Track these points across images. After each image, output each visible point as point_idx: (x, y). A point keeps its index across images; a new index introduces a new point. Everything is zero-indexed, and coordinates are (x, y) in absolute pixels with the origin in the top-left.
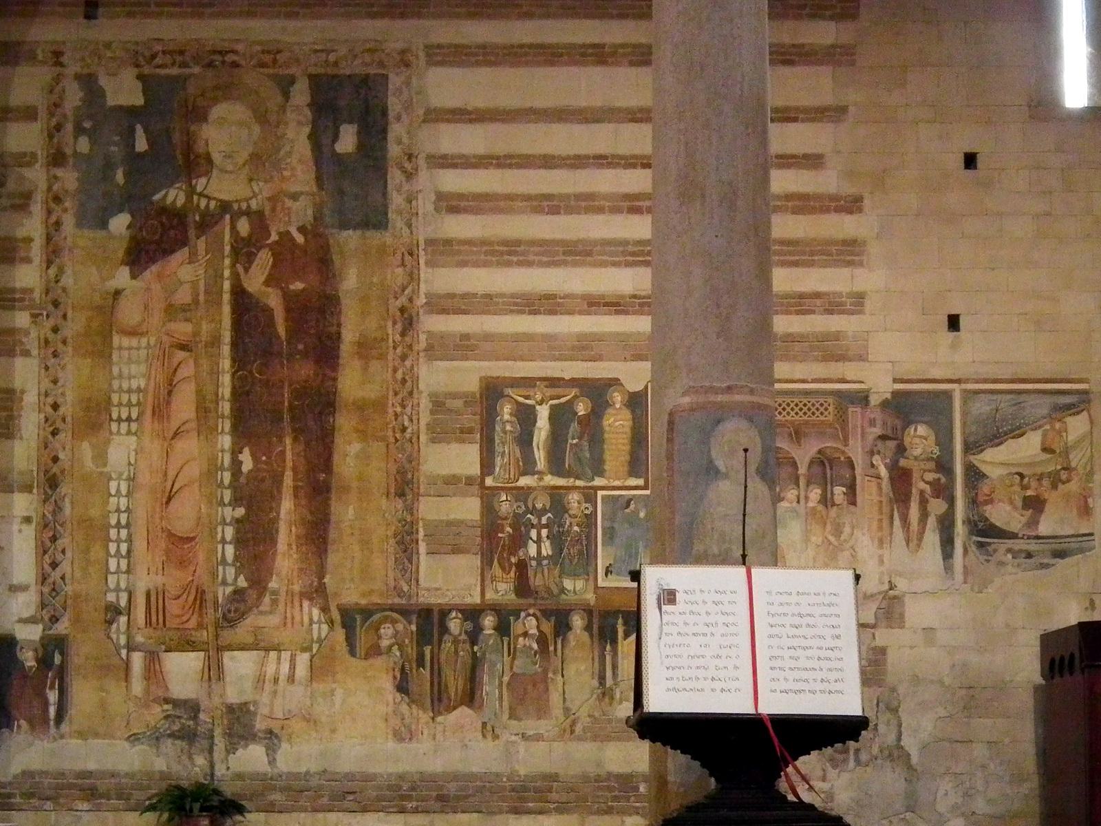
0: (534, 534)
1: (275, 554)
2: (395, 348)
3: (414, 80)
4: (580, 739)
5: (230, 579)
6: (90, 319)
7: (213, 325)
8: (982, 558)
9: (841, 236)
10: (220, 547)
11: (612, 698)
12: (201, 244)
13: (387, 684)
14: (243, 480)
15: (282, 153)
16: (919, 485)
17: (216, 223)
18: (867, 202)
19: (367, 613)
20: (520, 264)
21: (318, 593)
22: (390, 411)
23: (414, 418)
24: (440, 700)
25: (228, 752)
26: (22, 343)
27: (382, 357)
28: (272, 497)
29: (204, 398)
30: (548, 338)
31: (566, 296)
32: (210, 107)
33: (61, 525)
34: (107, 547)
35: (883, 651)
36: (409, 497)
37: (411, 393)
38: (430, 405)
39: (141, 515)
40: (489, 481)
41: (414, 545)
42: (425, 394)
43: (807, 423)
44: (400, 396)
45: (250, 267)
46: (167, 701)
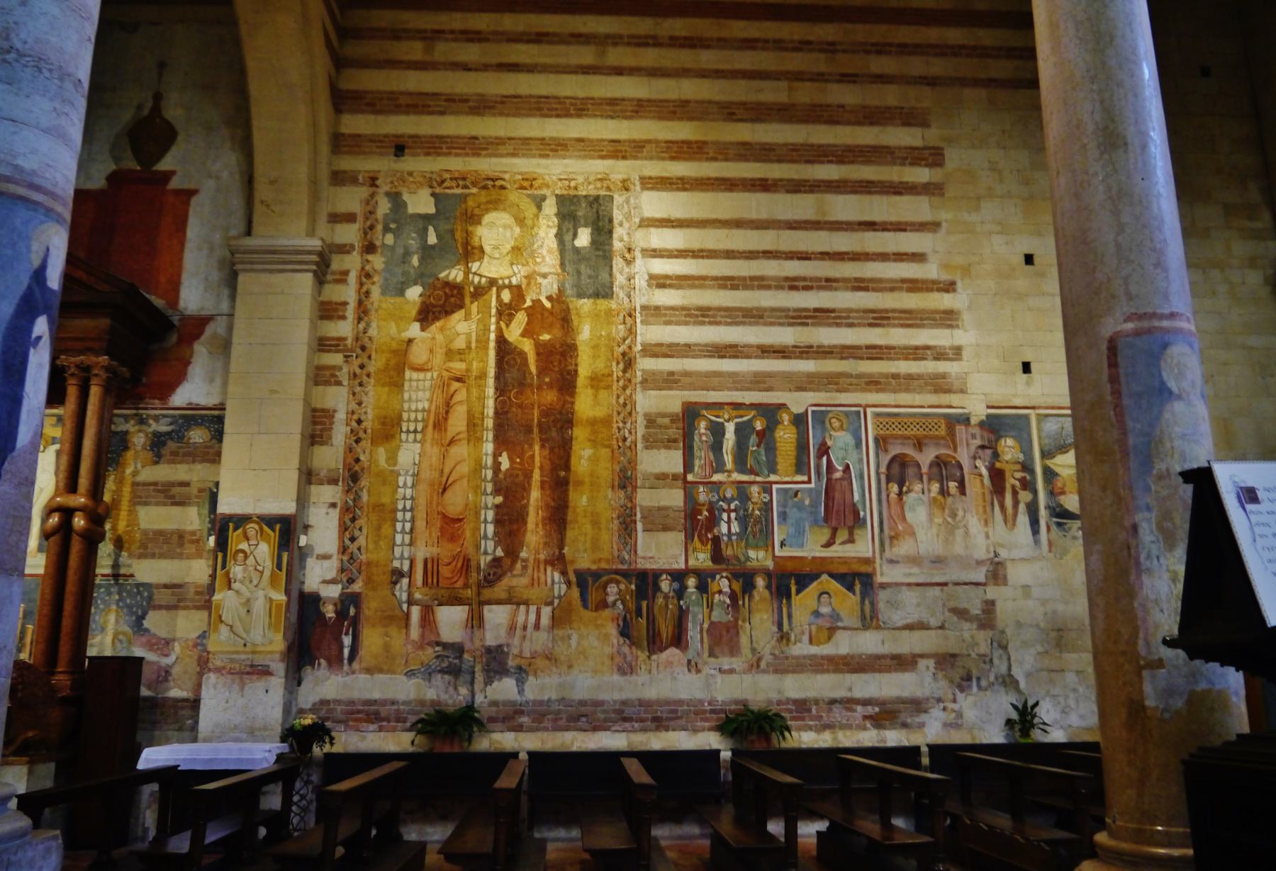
0: (725, 516)
1: (525, 531)
2: (618, 381)
3: (632, 201)
4: (764, 672)
5: (490, 550)
8: (1061, 534)
9: (942, 308)
10: (483, 525)
11: (788, 640)
12: (474, 308)
13: (612, 630)
14: (501, 476)
15: (535, 246)
16: (1011, 481)
18: (959, 285)
19: (596, 575)
20: (711, 323)
21: (558, 561)
22: (615, 426)
23: (633, 431)
24: (654, 643)
25: (486, 684)
26: (336, 376)
27: (608, 387)
28: (524, 489)
30: (733, 375)
31: (745, 346)
34: (394, 526)
35: (993, 603)
36: (629, 489)
37: (630, 414)
39: (422, 501)
40: (690, 477)
42: (641, 414)
43: (926, 437)
44: (622, 415)
46: (438, 644)
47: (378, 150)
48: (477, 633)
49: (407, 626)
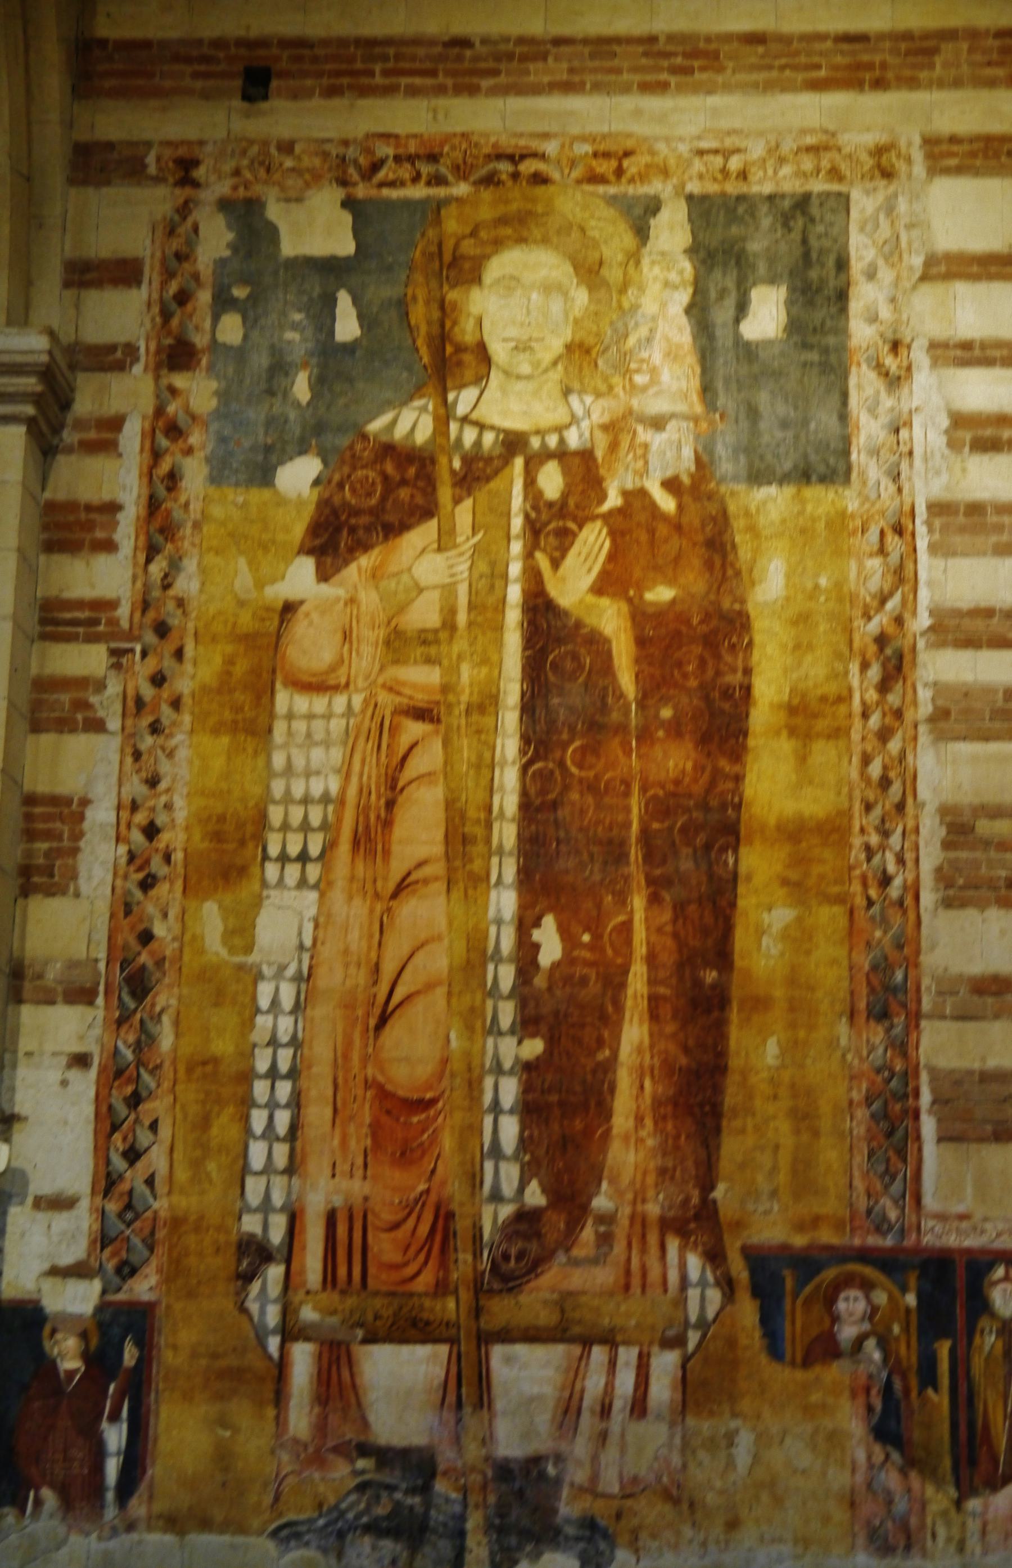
3: (902, 205)
5: (508, 1189)
6: (230, 661)
7: (484, 670)
10: (488, 1121)
12: (464, 514)
14: (540, 981)
15: (631, 341)
17: (497, 472)
22: (857, 841)
23: (909, 856)
24: (973, 1462)
26: (87, 706)
27: (838, 733)
28: (604, 1018)
29: (463, 816)
32: (487, 257)
33: (152, 1072)
34: (246, 1120)
36: (899, 1021)
37: (900, 807)
38: (943, 832)
41: (909, 1122)
44: (877, 812)
45: (563, 556)
46: (364, 1449)
47: (199, 84)
48: (471, 1419)
49: (280, 1397)
